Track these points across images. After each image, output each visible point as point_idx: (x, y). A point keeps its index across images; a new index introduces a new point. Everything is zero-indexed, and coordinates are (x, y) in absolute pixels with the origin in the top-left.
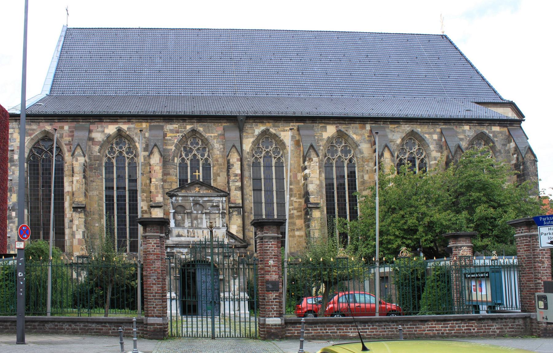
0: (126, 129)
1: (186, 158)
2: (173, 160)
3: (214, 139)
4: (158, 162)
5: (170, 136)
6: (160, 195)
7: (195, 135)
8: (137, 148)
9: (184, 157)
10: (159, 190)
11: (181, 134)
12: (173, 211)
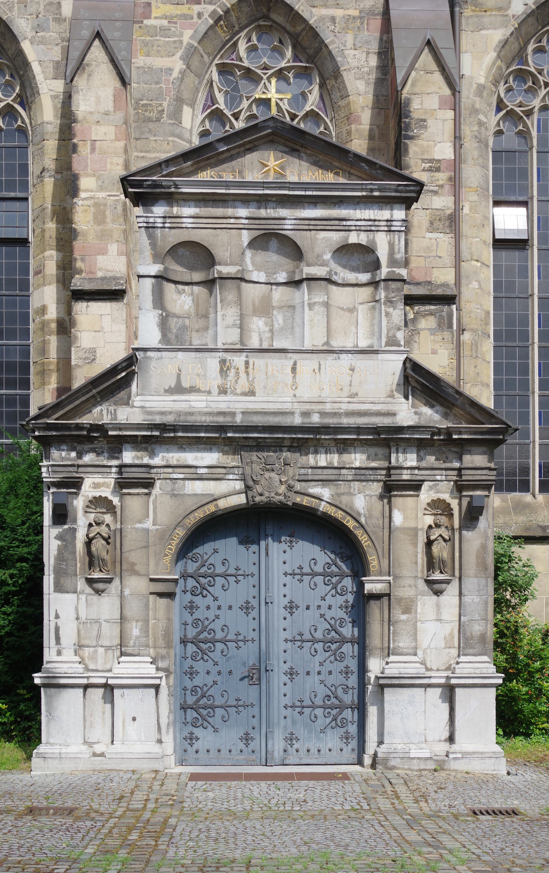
1: (228, 113)
2: (176, 115)
3: (346, 29)
4: (110, 106)
5: (165, 17)
6: (113, 248)
7: (266, 17)
8: (26, 64)
9: (222, 106)
10: (110, 225)
11: (211, 8)
12: (155, 269)
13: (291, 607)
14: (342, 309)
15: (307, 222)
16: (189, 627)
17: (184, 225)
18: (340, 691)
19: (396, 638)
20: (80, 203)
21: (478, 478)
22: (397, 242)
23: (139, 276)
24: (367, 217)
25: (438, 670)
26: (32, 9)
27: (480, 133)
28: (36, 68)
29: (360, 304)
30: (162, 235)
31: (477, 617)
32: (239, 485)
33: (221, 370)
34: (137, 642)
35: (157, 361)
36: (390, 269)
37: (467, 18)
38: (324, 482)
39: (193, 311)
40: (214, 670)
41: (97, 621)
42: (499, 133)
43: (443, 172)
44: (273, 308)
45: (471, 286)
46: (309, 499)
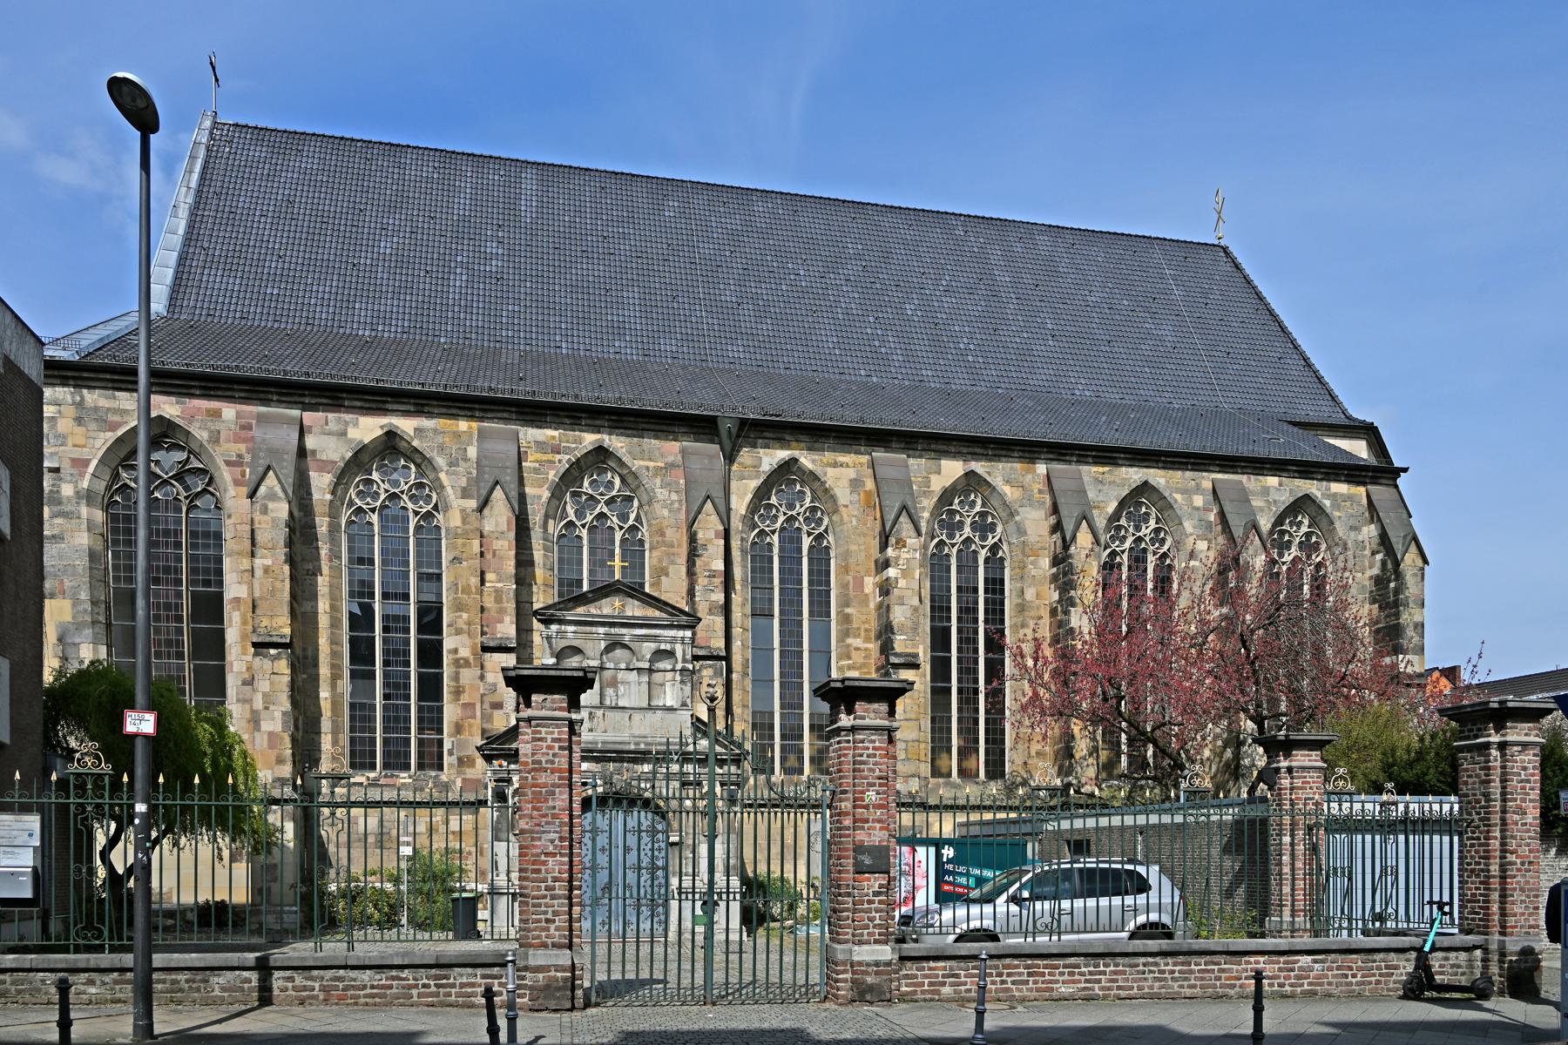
1: (578, 524)
3: (655, 475)
4: (505, 528)
8: (443, 487)
11: (567, 457)
28: (449, 490)
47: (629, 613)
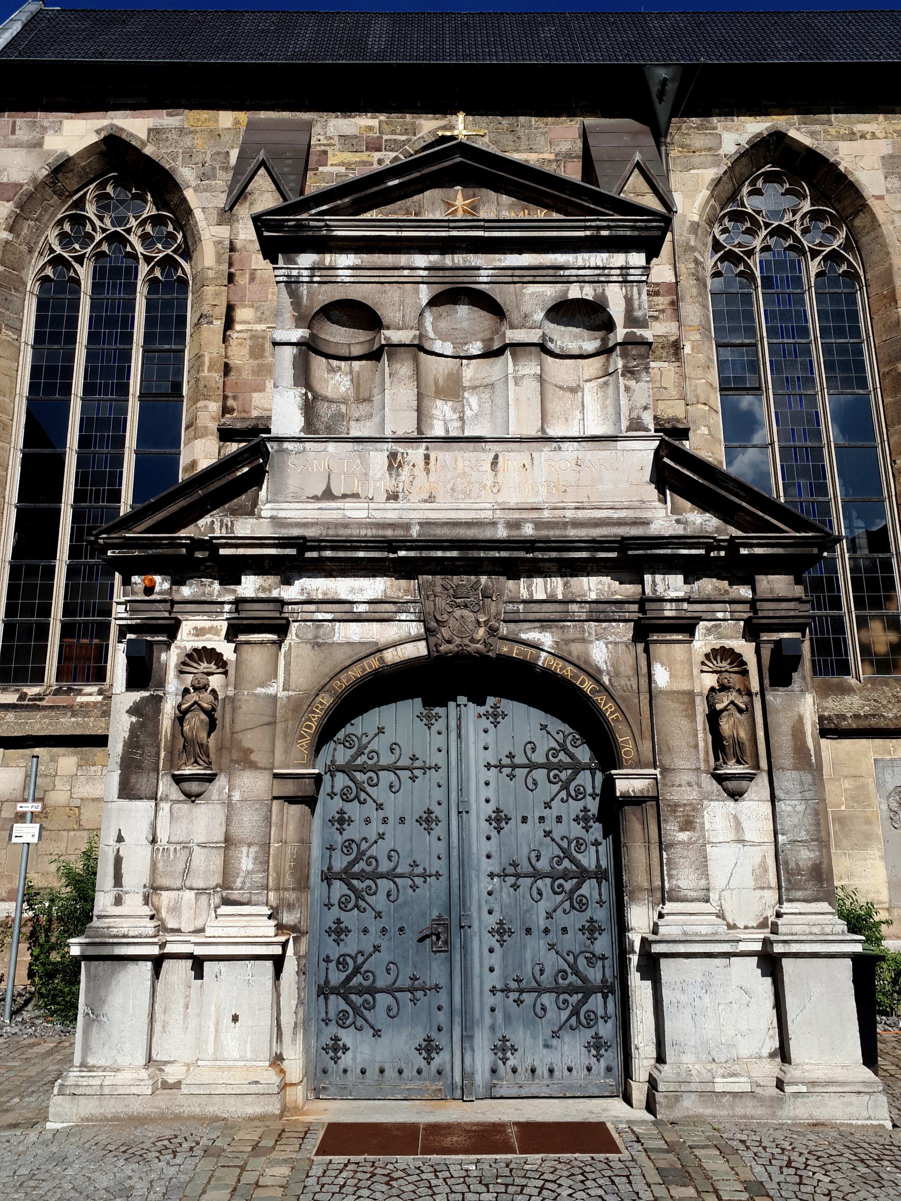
0: (143, 136)
5: (342, 164)
8: (189, 212)
11: (393, 155)
12: (297, 334)
13: (498, 819)
14: (561, 388)
15: (509, 272)
16: (337, 855)
17: (339, 279)
18: (582, 963)
19: (674, 872)
20: (235, 335)
21: (783, 613)
22: (636, 296)
23: (275, 344)
24: (593, 265)
25: (746, 928)
26: (198, 158)
27: (698, 272)
28: (198, 214)
29: (586, 381)
30: (309, 293)
31: (803, 836)
32: (416, 629)
33: (390, 466)
34: (248, 880)
35: (298, 455)
36: (628, 330)
37: (675, 158)
38: (544, 623)
39: (351, 393)
40: (374, 927)
41: (186, 846)
42: (717, 274)
43: (663, 296)
44: (464, 389)
45: (699, 432)
46: (523, 648)
47: (486, 213)
